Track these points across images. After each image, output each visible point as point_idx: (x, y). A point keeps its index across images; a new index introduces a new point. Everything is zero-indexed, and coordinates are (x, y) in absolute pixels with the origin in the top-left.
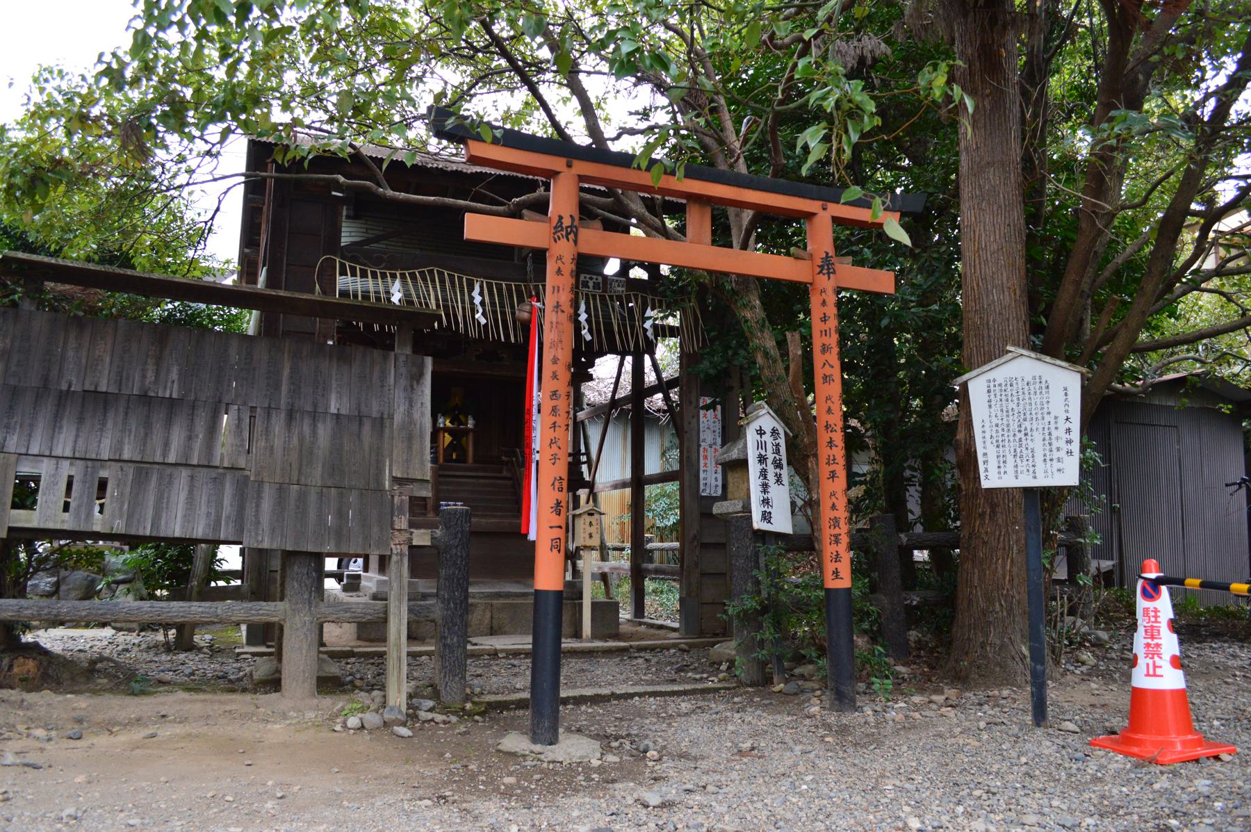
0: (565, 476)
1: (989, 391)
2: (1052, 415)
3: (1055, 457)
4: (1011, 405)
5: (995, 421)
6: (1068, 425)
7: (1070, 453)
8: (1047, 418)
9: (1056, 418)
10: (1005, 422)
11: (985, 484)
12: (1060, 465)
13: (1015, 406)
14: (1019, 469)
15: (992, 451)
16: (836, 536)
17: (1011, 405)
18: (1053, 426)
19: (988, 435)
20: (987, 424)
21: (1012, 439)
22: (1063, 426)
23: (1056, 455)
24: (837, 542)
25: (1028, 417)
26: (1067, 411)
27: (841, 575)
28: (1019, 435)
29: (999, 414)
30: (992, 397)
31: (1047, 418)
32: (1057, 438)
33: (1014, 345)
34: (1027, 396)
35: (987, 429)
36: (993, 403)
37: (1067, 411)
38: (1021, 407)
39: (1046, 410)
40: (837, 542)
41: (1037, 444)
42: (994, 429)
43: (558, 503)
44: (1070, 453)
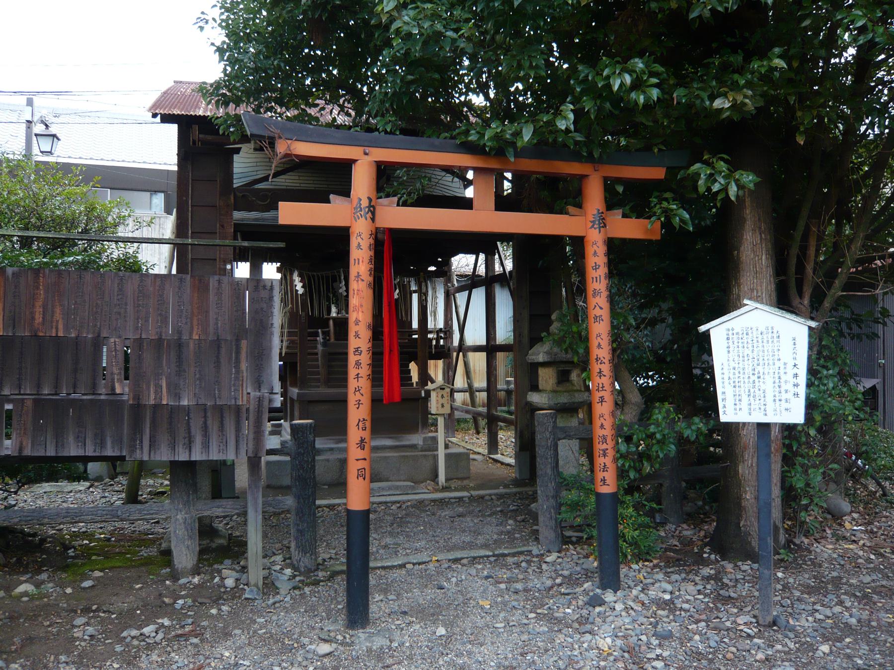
0: (368, 418)
1: (728, 339)
2: (782, 362)
3: (783, 398)
4: (747, 352)
5: (732, 364)
6: (795, 371)
7: (796, 395)
8: (778, 364)
9: (785, 364)
10: (741, 365)
11: (723, 418)
12: (787, 405)
13: (750, 353)
14: (753, 407)
15: (729, 391)
16: (605, 451)
17: (747, 352)
18: (782, 371)
19: (726, 377)
20: (726, 367)
21: (747, 380)
22: (791, 371)
23: (784, 396)
24: (605, 455)
25: (761, 362)
26: (795, 359)
27: (608, 482)
28: (753, 378)
29: (736, 358)
30: (731, 344)
31: (778, 364)
32: (786, 382)
33: (750, 299)
34: (760, 344)
35: (725, 371)
36: (731, 349)
37: (795, 359)
38: (755, 352)
39: (776, 357)
40: (605, 455)
41: (768, 385)
42: (732, 371)
43: (362, 440)
44: (796, 395)
